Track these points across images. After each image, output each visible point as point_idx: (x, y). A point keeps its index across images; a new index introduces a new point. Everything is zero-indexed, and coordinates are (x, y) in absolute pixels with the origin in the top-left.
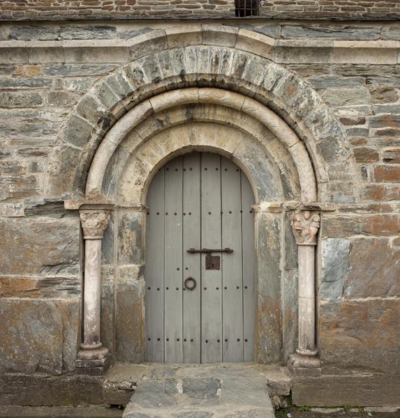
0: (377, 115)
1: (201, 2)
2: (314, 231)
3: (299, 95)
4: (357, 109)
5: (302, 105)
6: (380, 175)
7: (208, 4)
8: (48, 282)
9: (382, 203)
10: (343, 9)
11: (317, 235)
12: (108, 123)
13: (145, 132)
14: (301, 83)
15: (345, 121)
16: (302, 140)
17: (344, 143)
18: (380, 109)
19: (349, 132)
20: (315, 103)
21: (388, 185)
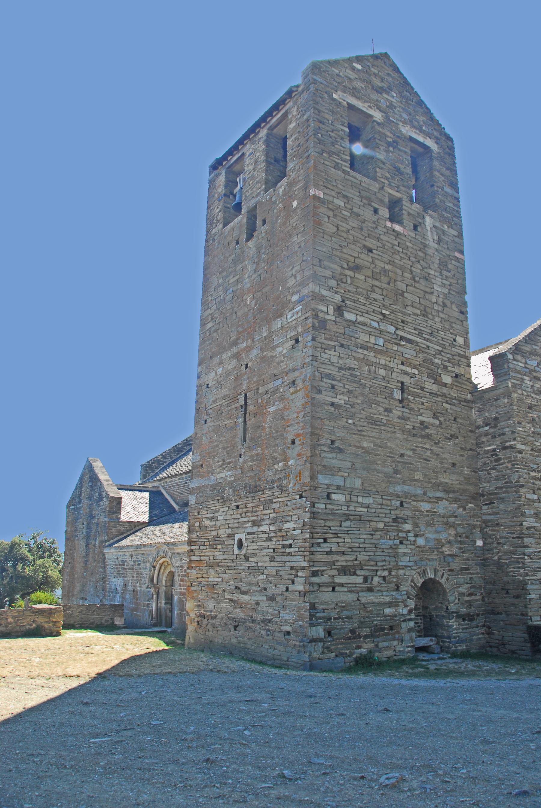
8: (148, 604)
12: (155, 567)
13: (163, 567)
21: (182, 583)
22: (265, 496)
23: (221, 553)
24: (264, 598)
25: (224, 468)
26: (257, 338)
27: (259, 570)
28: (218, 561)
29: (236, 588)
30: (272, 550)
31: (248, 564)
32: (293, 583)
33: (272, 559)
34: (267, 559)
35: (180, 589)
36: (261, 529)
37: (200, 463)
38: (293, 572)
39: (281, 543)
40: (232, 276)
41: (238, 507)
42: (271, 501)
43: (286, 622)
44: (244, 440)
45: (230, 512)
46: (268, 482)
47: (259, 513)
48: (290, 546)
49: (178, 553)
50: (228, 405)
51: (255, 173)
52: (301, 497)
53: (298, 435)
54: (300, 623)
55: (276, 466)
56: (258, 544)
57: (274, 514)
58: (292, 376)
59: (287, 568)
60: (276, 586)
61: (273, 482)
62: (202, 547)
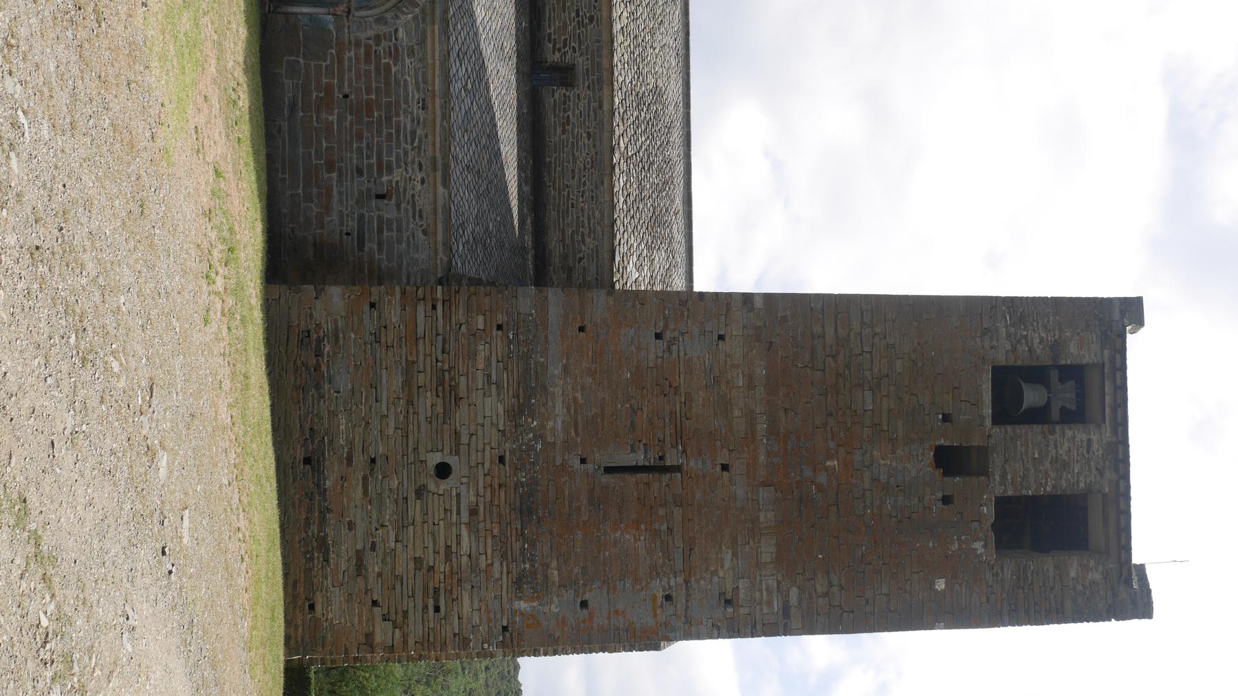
0: (399, 47)
1: (554, 31)
2: (338, 13)
3: (409, 8)
4: (403, 38)
5: (404, 9)
6: (368, 47)
7: (553, 37)
9: (353, 48)
10: (550, 162)
11: (336, 15)
14: (416, 9)
15: (396, 30)
16: (386, 11)
17: (384, 29)
18: (403, 49)
19: (390, 32)
20: (405, 16)
21: (362, 50)
22: (514, 538)
23: (429, 414)
24: (359, 546)
25: (569, 411)
26: (765, 494)
27: (402, 524)
28: (415, 402)
29: (373, 461)
30: (431, 564)
31: (412, 496)
32: (385, 618)
33: (418, 561)
34: (419, 554)
35: (350, 42)
36: (464, 533)
37: (589, 327)
38: (400, 619)
39: (442, 585)
40: (892, 406)
41: (502, 460)
42: (504, 556)
43: (329, 602)
44: (609, 470)
45: (495, 436)
46: (533, 545)
47: (488, 526)
48: (437, 609)
49: (422, 42)
50: (672, 413)
51: (1048, 465)
52: (505, 629)
53: (591, 615)
54: (329, 638)
55: (554, 564)
56: (441, 522)
57: (483, 566)
58: (680, 601)
59: (405, 603)
60: (380, 575)
61: (532, 561)
62: (440, 338)
